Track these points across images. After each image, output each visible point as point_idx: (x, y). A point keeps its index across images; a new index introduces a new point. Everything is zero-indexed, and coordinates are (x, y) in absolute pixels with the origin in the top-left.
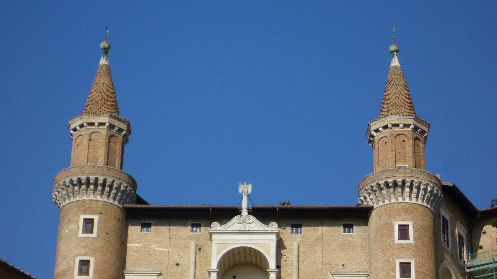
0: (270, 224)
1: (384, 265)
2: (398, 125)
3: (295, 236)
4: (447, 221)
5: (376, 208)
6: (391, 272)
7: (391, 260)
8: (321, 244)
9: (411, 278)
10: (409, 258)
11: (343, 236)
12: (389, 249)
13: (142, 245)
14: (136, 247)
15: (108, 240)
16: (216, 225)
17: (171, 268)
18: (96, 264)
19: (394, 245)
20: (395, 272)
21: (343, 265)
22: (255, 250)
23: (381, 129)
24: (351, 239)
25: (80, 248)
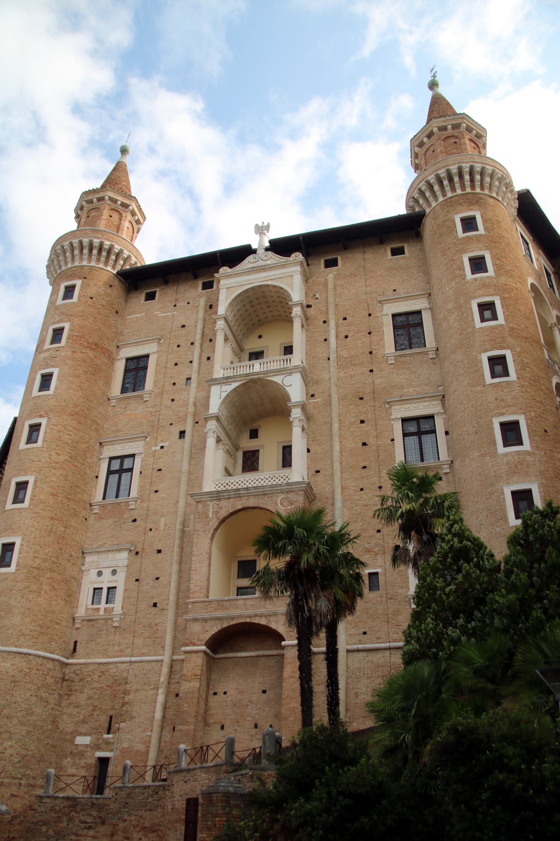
0: (293, 255)
1: (447, 268)
2: (444, 129)
3: (328, 271)
4: (527, 244)
5: (430, 212)
6: (458, 272)
7: (456, 257)
8: (363, 273)
9: (504, 447)
10: (481, 250)
11: (391, 260)
12: (452, 247)
13: (143, 314)
14: (137, 317)
15: (92, 304)
16: (224, 270)
17: (175, 331)
18: (71, 330)
19: (457, 240)
20: (464, 270)
21: (395, 290)
22: (275, 287)
23: (425, 140)
24: (403, 261)
25: (56, 316)
